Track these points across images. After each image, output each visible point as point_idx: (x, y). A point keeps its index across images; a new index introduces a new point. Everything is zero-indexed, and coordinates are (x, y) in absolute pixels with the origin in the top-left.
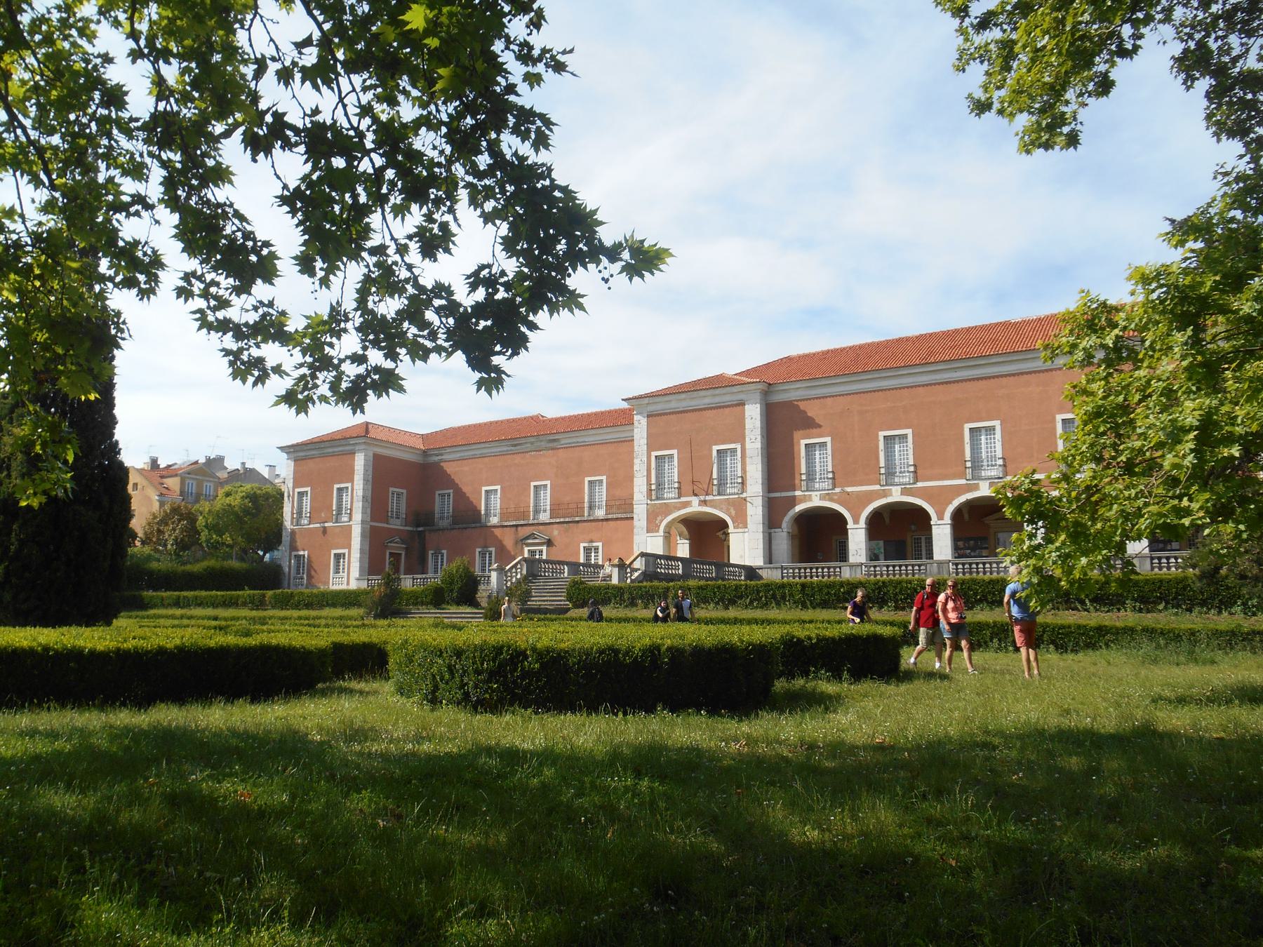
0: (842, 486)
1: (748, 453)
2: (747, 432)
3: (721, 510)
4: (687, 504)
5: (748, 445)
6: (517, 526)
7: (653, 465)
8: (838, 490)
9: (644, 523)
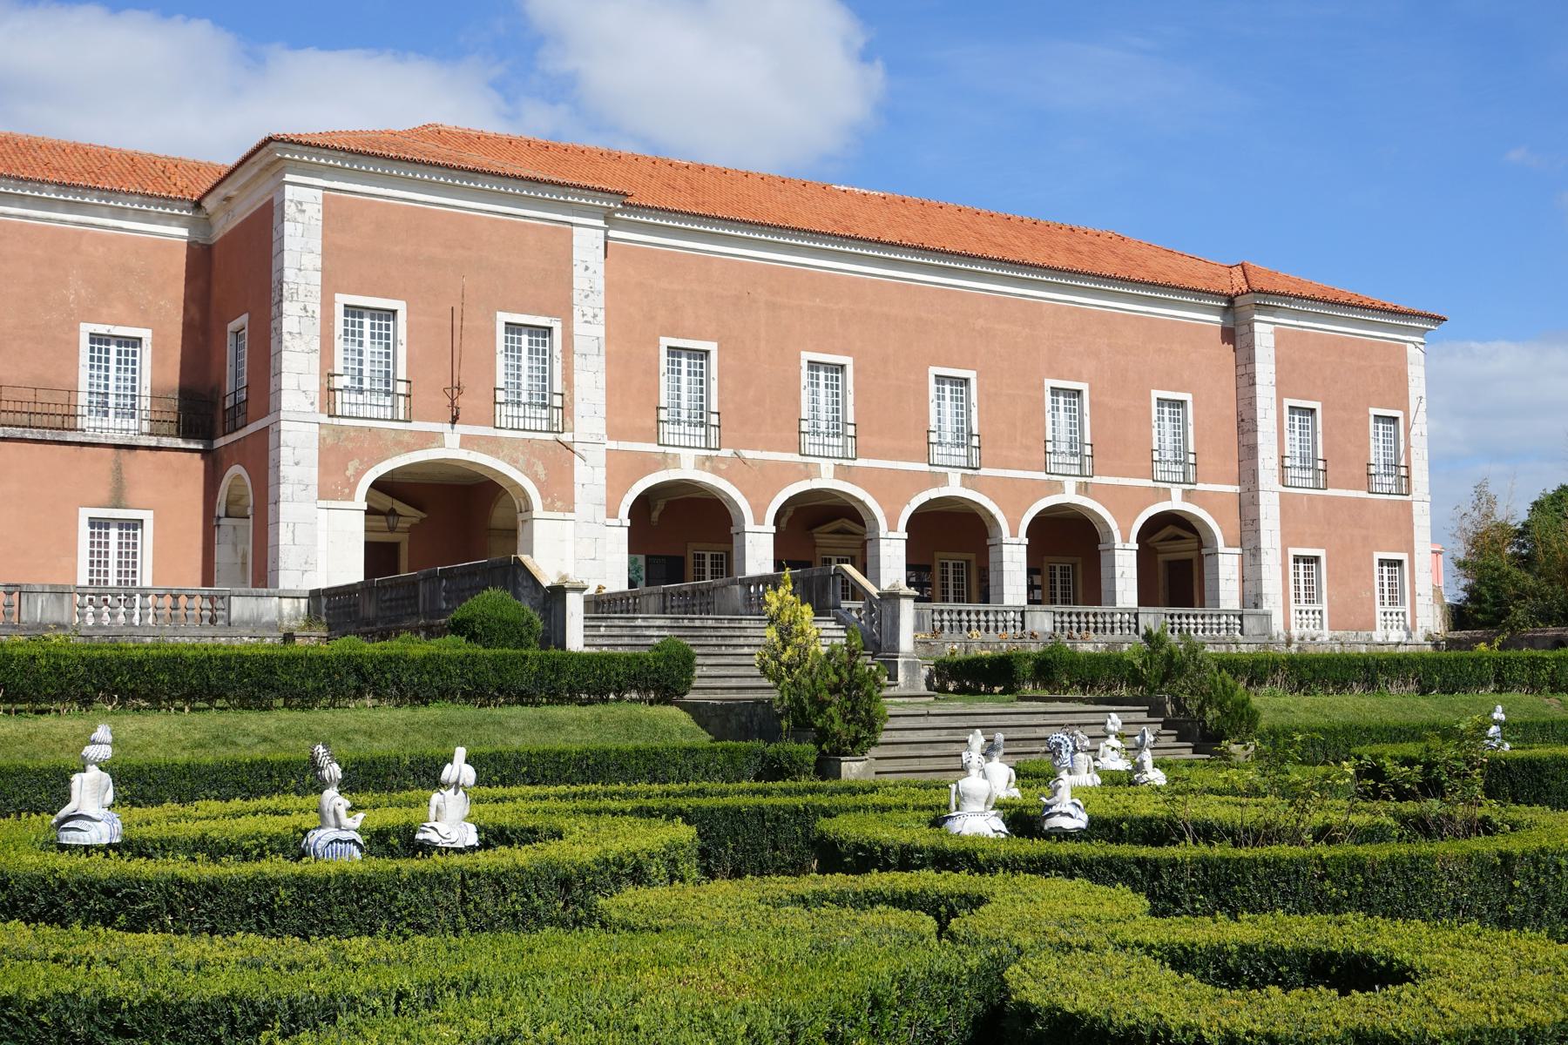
0: (736, 447)
1: (579, 344)
2: (576, 298)
3: (513, 462)
5: (578, 327)
8: (726, 452)
9: (312, 473)
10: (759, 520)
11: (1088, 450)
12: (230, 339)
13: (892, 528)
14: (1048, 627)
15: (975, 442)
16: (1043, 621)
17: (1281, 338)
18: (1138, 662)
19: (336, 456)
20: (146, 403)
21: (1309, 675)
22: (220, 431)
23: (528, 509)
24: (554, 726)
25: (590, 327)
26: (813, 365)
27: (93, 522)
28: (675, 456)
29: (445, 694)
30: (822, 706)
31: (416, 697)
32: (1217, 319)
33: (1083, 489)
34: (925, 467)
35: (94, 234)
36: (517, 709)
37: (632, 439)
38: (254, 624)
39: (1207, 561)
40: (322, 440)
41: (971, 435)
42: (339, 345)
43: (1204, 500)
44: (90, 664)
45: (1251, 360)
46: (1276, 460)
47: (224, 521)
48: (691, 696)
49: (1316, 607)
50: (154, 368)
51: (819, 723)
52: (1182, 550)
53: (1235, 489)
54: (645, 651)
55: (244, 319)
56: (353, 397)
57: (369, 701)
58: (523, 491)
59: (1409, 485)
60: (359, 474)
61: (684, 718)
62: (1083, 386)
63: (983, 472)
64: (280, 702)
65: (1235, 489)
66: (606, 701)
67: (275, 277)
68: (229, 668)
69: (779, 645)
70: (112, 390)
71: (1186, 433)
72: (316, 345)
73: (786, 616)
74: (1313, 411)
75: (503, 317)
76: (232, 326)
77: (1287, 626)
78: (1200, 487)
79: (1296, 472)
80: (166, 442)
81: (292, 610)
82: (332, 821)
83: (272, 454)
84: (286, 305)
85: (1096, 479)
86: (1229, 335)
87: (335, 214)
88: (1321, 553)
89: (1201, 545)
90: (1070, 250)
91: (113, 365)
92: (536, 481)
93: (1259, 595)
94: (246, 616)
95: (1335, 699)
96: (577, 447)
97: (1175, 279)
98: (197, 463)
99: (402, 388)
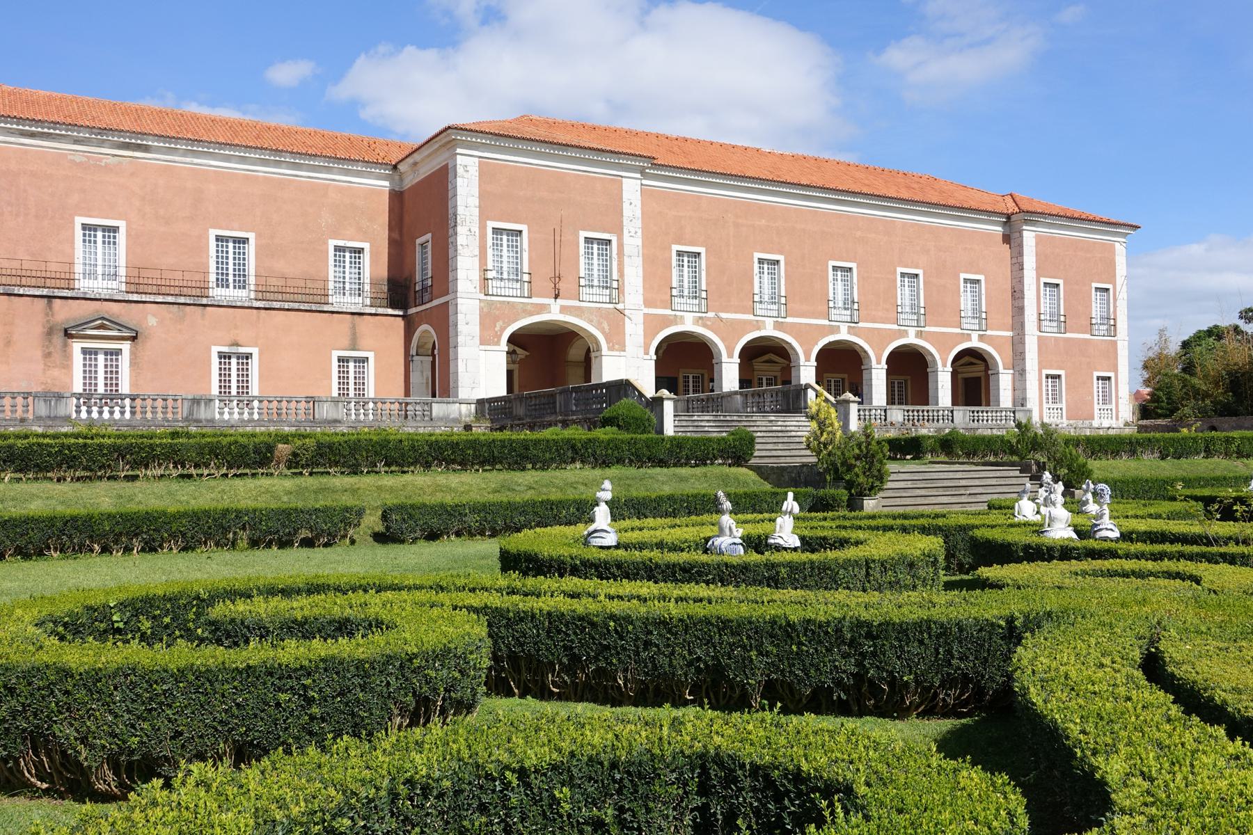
0: (717, 311)
1: (627, 250)
3: (590, 322)
4: (542, 308)
5: (627, 239)
6: (50, 298)
7: (490, 242)
8: (711, 314)
9: (475, 329)
10: (730, 355)
11: (922, 311)
12: (418, 249)
13: (808, 359)
14: (900, 419)
15: (856, 306)
16: (897, 414)
17: (1039, 240)
18: (1014, 441)
19: (489, 318)
20: (367, 287)
21: (1097, 448)
22: (412, 303)
23: (599, 349)
24: (682, 479)
25: (633, 240)
26: (761, 261)
27: (340, 360)
28: (682, 317)
29: (620, 461)
30: (850, 468)
31: (604, 462)
32: (1000, 229)
33: (919, 335)
34: (826, 322)
35: (336, 186)
36: (658, 470)
37: (656, 307)
38: (446, 419)
39: (992, 378)
40: (481, 309)
41: (853, 302)
42: (490, 252)
43: (990, 340)
44: (430, 445)
45: (1021, 254)
46: (1035, 316)
47: (415, 358)
48: (753, 461)
49: (1059, 406)
50: (373, 266)
51: (848, 477)
52: (976, 371)
53: (1010, 334)
54: (724, 434)
55: (429, 236)
56: (498, 283)
57: (578, 465)
58: (596, 338)
59: (1115, 330)
60: (503, 330)
61: (752, 475)
62: (920, 272)
63: (861, 325)
64: (530, 466)
65: (1010, 334)
66: (705, 464)
67: (451, 211)
68: (504, 447)
69: (819, 433)
70: (347, 280)
71: (980, 299)
72: (477, 253)
73: (822, 416)
74: (1058, 285)
75: (583, 234)
76: (419, 241)
77: (1041, 417)
78: (989, 333)
79: (1048, 323)
80: (380, 311)
81: (466, 411)
82: (728, 532)
83: (451, 319)
84: (459, 229)
85: (927, 329)
86: (1007, 239)
87: (486, 173)
88: (1062, 372)
89: (987, 368)
90: (908, 188)
91: (347, 264)
92: (603, 332)
93: (1024, 399)
94: (441, 414)
95: (1111, 461)
96: (626, 312)
97: (974, 205)
98: (400, 323)
99: (526, 278)
